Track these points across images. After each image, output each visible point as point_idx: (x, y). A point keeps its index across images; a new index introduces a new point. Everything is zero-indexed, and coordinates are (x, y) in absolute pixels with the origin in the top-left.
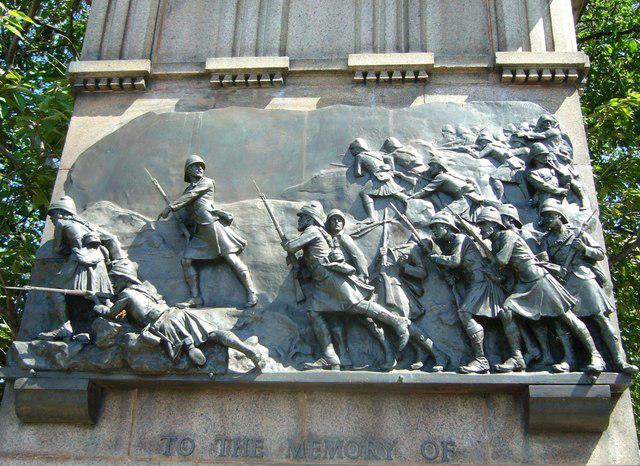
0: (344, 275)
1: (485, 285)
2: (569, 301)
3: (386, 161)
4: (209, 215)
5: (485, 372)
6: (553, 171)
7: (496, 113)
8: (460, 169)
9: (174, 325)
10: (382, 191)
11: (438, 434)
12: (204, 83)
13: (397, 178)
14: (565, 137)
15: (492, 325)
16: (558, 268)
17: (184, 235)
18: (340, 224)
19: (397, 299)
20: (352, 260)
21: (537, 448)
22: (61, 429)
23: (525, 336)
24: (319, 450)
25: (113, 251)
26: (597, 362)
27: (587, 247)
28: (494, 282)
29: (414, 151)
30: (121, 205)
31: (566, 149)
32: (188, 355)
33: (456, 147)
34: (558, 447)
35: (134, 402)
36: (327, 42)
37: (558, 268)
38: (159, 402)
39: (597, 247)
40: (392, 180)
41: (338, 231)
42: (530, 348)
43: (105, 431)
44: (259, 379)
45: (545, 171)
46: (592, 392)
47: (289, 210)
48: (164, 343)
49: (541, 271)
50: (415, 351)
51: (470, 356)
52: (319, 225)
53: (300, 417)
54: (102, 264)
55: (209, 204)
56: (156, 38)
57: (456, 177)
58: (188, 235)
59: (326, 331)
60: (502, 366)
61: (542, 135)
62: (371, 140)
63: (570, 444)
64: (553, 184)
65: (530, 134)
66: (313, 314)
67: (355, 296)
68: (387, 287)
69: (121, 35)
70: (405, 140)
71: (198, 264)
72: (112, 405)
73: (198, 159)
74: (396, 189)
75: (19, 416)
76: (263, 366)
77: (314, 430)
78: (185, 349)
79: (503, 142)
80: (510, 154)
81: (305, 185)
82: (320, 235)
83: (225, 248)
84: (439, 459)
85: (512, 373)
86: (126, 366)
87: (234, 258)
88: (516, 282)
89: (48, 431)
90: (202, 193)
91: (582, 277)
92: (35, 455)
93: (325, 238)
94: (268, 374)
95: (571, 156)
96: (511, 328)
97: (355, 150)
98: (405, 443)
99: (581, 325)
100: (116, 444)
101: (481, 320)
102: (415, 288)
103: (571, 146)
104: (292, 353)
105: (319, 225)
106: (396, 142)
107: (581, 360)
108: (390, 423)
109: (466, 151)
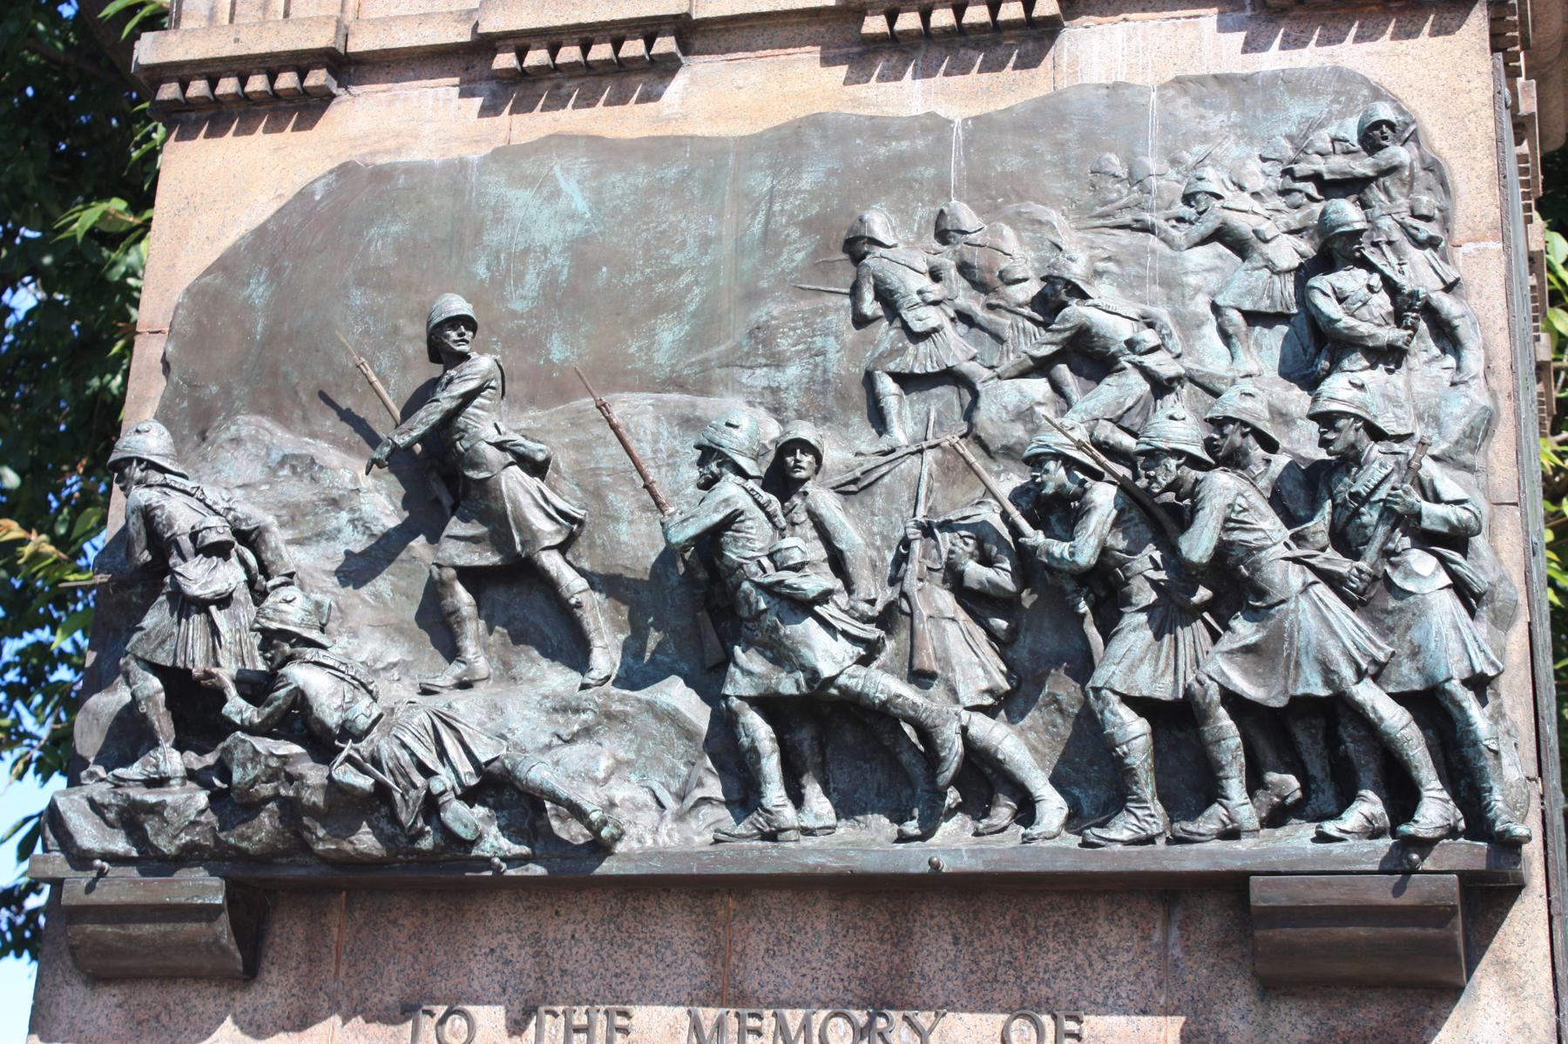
0: (804, 606)
2: (1365, 654)
3: (935, 275)
4: (492, 454)
5: (1150, 840)
6: (1375, 280)
7: (1242, 108)
8: (1128, 285)
9: (404, 746)
10: (919, 359)
13: (964, 317)
14: (1433, 167)
15: (1175, 720)
16: (1343, 566)
17: (437, 501)
18: (806, 460)
19: (945, 661)
20: (837, 562)
25: (268, 556)
26: (1435, 809)
27: (1427, 508)
29: (1009, 239)
30: (286, 423)
31: (1426, 202)
33: (1127, 218)
37: (1343, 566)
38: (395, 922)
40: (948, 326)
41: (803, 481)
44: (608, 867)
45: (1352, 280)
46: (1418, 891)
47: (689, 423)
48: (381, 790)
49: (1296, 577)
52: (746, 476)
54: (243, 594)
55: (485, 427)
57: (1109, 313)
58: (447, 501)
60: (1191, 827)
61: (1362, 166)
62: (902, 213)
64: (1372, 319)
65: (1337, 165)
67: (829, 655)
68: (919, 626)
70: (990, 211)
72: (288, 934)
73: (457, 305)
74: (955, 348)
76: (616, 839)
78: (431, 806)
79: (1255, 195)
80: (1268, 229)
81: (734, 350)
83: (531, 537)
85: (1216, 845)
87: (552, 562)
90: (468, 398)
91: (1409, 586)
93: (762, 507)
94: (628, 857)
95: (1445, 222)
97: (857, 246)
99: (1395, 719)
101: (1142, 705)
103: (1447, 191)
104: (689, 802)
105: (746, 476)
106: (966, 216)
107: (1402, 796)
108: (931, 966)
109: (1148, 229)
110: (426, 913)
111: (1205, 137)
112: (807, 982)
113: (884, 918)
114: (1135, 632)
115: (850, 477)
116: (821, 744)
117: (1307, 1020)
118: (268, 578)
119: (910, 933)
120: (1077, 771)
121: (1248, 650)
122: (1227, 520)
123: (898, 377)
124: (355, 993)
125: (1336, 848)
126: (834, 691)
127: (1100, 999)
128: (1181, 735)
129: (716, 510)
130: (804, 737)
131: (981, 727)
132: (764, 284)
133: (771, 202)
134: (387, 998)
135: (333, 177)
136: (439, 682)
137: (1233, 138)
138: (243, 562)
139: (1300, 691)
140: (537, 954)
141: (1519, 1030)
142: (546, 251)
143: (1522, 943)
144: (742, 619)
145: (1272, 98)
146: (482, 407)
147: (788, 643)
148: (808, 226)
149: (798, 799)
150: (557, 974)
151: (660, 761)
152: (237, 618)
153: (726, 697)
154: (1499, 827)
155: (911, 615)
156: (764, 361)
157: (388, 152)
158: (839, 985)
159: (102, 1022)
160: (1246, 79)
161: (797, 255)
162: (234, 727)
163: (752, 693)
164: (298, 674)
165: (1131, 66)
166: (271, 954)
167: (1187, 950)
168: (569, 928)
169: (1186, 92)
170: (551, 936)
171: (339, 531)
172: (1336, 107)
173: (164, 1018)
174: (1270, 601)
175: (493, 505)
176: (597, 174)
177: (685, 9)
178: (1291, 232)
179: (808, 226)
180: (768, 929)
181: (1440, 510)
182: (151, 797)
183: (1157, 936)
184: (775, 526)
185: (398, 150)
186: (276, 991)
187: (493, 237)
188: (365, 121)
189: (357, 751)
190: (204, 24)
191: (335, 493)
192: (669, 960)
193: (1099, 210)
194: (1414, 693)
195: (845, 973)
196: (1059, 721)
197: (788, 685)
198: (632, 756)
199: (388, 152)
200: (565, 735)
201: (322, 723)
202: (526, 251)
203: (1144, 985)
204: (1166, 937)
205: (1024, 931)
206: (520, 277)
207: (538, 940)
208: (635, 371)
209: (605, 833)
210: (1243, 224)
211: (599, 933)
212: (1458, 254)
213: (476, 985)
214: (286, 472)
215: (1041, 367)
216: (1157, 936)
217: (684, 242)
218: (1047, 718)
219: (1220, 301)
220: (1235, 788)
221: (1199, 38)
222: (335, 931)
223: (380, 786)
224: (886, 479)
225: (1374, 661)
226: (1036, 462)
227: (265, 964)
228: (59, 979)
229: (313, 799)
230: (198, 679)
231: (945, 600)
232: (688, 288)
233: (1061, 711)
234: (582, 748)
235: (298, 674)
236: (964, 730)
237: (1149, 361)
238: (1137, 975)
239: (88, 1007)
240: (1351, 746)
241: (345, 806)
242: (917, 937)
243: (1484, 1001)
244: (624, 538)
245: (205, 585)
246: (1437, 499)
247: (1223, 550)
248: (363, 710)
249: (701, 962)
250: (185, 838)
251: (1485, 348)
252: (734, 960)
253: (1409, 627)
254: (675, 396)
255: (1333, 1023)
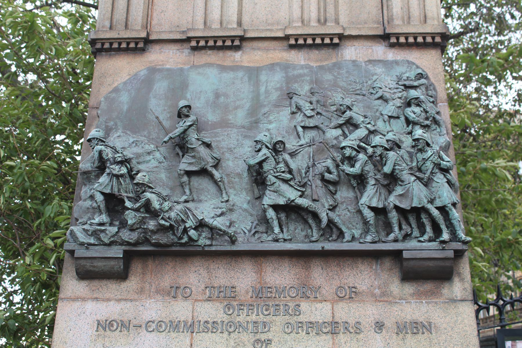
1: (376, 186)
11: (346, 281)
12: (185, 45)
17: (178, 154)
21: (409, 288)
22: (104, 282)
23: (402, 219)
24: (271, 292)
28: (382, 185)
32: (187, 234)
33: (358, 92)
34: (422, 289)
35: (151, 264)
36: (270, 16)
39: (448, 161)
42: (404, 227)
43: (132, 283)
50: (331, 229)
51: (366, 232)
52: (269, 149)
53: (259, 272)
56: (150, 13)
58: (181, 154)
59: (274, 217)
63: (428, 286)
66: (266, 206)
69: (125, 10)
71: (189, 173)
75: (77, 273)
77: (268, 280)
79: (389, 89)
82: (269, 155)
84: (347, 297)
86: (146, 241)
88: (396, 185)
89: (96, 283)
92: (88, 299)
96: (394, 216)
98: (326, 288)
99: (436, 213)
100: (141, 291)
102: (331, 188)
104: (253, 232)
105: (269, 149)
109: (364, 95)
110: (176, 261)
111: (376, 74)
112: (283, 279)
113: (303, 263)
114: (370, 190)
115: (292, 151)
116: (287, 217)
117: (412, 287)
118: (132, 171)
119: (310, 267)
120: (353, 226)
121: (401, 195)
122: (395, 163)
123: (303, 127)
124: (157, 282)
125: (424, 244)
126: (294, 204)
127: (360, 283)
128: (380, 217)
129: (262, 156)
130: (283, 216)
131: (331, 214)
132: (265, 103)
133: (267, 83)
134: (166, 284)
135: (145, 70)
136: (180, 200)
137: (383, 75)
138: (126, 167)
139: (413, 205)
140: (208, 272)
141: (464, 289)
142: (206, 92)
143: (463, 268)
144: (267, 185)
145: (392, 66)
146: (193, 129)
147: (282, 191)
148: (277, 89)
149: (282, 231)
150: (214, 277)
151: (244, 222)
152: (126, 181)
153: (264, 205)
154: (463, 239)
155: (311, 185)
156: (266, 122)
157: (160, 65)
158: (292, 280)
159: (82, 290)
160: (386, 61)
161: (274, 96)
162: (128, 209)
163: (272, 204)
164: (148, 195)
165: (356, 57)
166: (131, 272)
167: (382, 271)
168: (217, 266)
169: (371, 64)
170: (212, 267)
171: (150, 161)
172: (408, 70)
173: (100, 289)
174: (405, 183)
175: (196, 154)
176: (219, 74)
177: (243, 34)
178: (399, 98)
179: (277, 89)
180: (272, 266)
181: (445, 163)
182: (103, 228)
183: (374, 267)
184: (276, 162)
185: (163, 65)
186: (134, 282)
187: (191, 88)
188: (156, 56)
189: (165, 216)
190: (108, 29)
191: (149, 151)
192: (245, 274)
193: (351, 90)
194: (440, 207)
195: (293, 277)
196: (348, 213)
197: (281, 201)
198: (236, 220)
199: (160, 65)
200: (218, 213)
201: (155, 208)
202: (201, 92)
203: (371, 279)
204: (376, 267)
205: (340, 266)
206: (199, 98)
207: (208, 269)
208: (231, 123)
209: (233, 239)
210: (387, 95)
211: (225, 267)
212: (438, 105)
213: (191, 280)
214: (134, 145)
215: (340, 126)
216: (374, 267)
217: (244, 92)
218: (345, 213)
219: (383, 113)
220: (396, 229)
221: (373, 51)
222: (150, 266)
223: (171, 224)
224: (302, 152)
225: (431, 199)
226: (343, 148)
227: (130, 275)
228: (69, 279)
229: (153, 228)
230: (117, 196)
231: (319, 183)
232: (245, 103)
233: (349, 211)
234: (222, 218)
235: (148, 195)
236: (327, 214)
237: (369, 126)
238: (369, 277)
239: (78, 286)
240: (424, 220)
241: (162, 229)
242: (312, 268)
243: (455, 282)
244: (231, 165)
245: (118, 171)
246: (443, 160)
247: (394, 170)
248: (166, 205)
249: (254, 274)
250: (112, 239)
251: (446, 128)
252: (263, 274)
253: (438, 191)
254: (243, 130)
255: (419, 288)
